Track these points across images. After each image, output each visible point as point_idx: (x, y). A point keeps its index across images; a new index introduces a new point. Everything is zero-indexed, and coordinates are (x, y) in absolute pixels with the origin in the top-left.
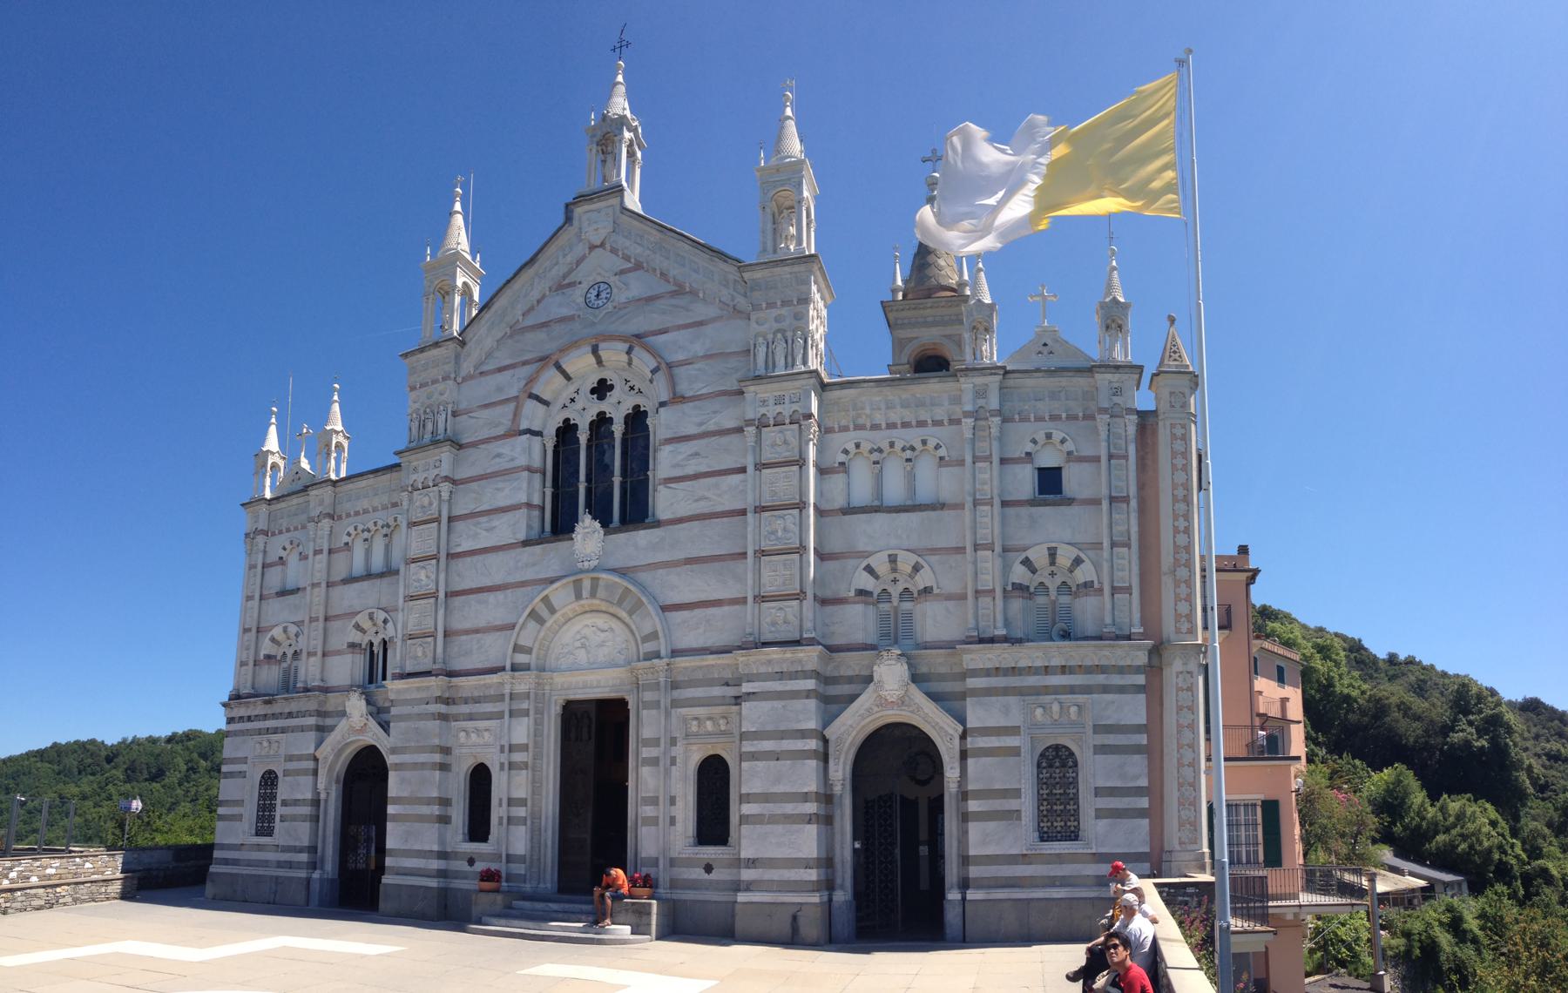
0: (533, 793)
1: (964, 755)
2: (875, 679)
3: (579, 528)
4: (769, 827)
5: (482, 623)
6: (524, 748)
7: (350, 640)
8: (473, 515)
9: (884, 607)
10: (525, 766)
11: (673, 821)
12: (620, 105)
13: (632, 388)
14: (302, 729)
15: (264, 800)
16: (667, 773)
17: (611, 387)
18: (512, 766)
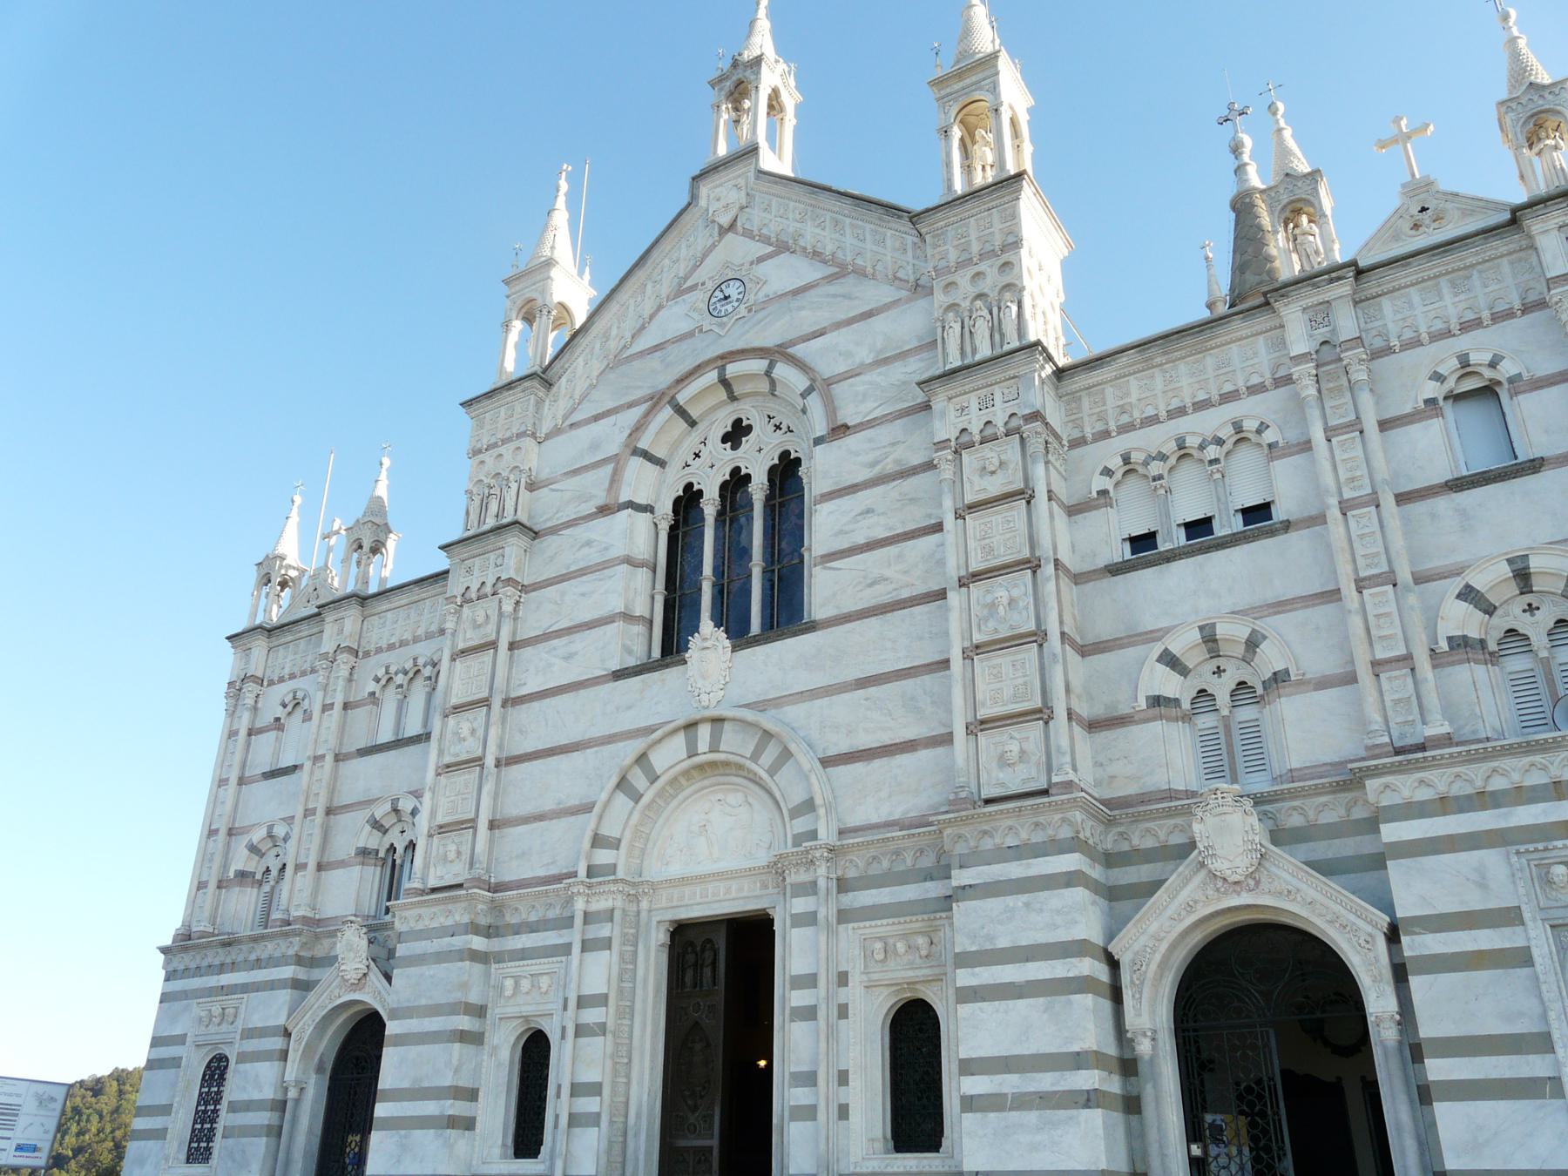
0: (615, 1073)
2: (1200, 846)
3: (695, 642)
5: (549, 805)
6: (602, 1000)
7: (361, 844)
8: (546, 637)
9: (1206, 721)
10: (601, 1029)
11: (843, 1112)
12: (762, 41)
13: (778, 427)
14: (272, 985)
15: (206, 1104)
16: (832, 1035)
17: (749, 428)
18: (580, 1031)
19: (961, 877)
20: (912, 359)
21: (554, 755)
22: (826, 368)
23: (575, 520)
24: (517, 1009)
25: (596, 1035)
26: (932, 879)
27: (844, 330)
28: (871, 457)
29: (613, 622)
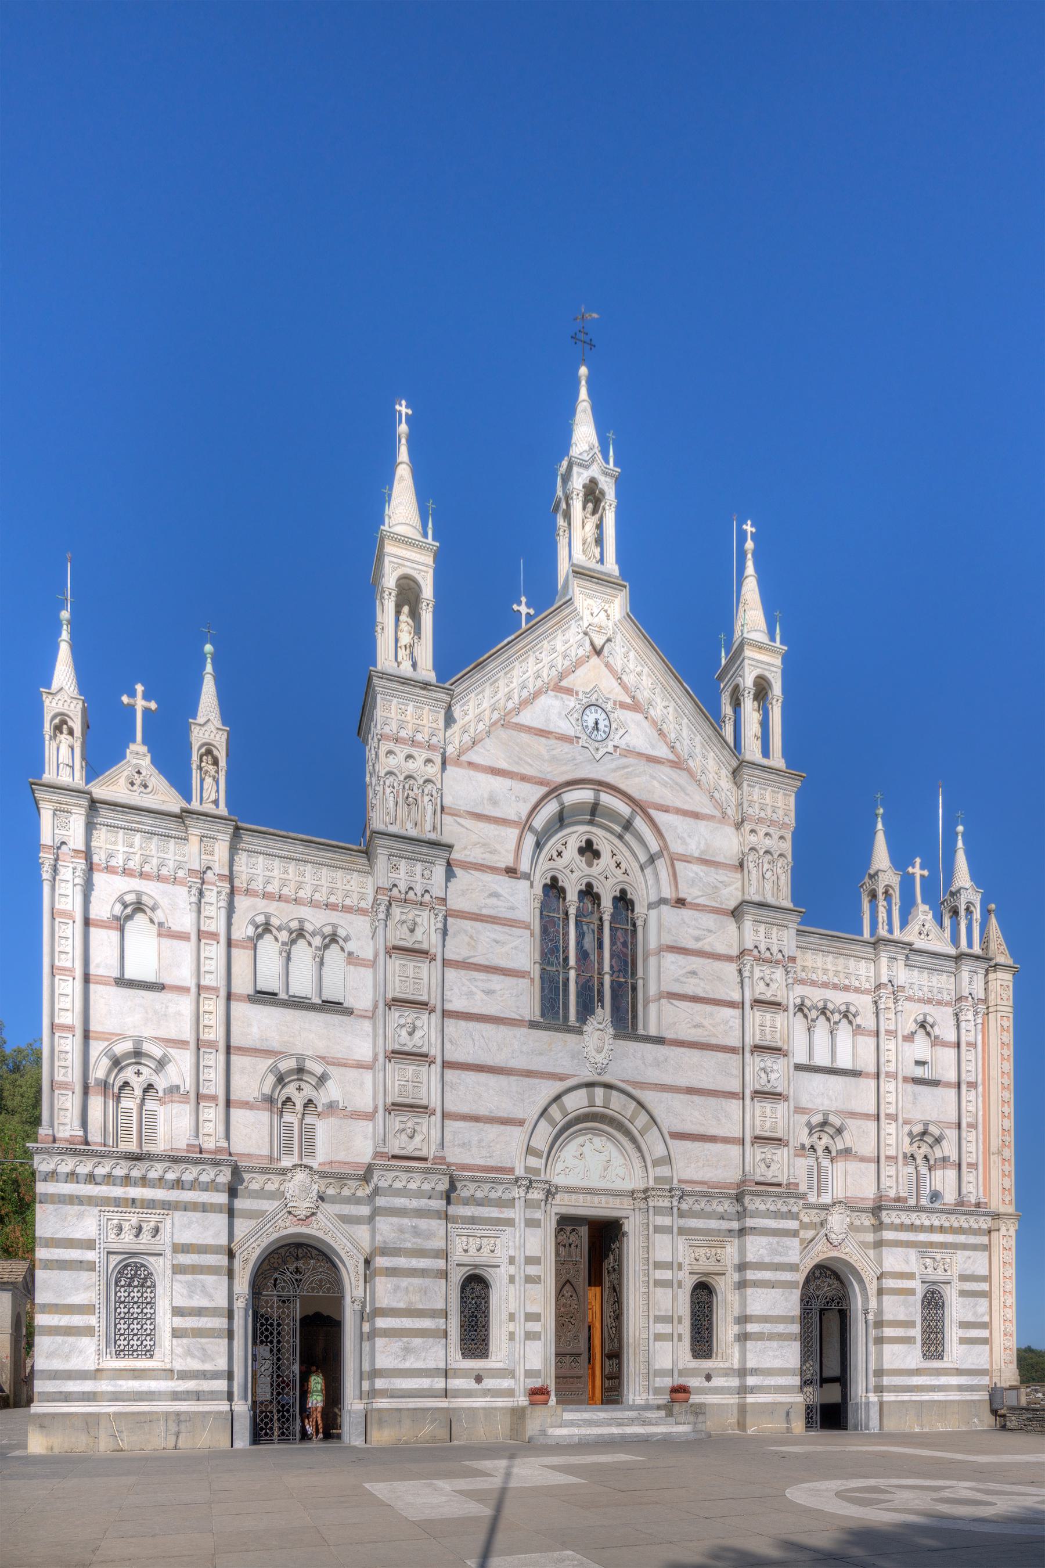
1: (880, 1292)
4: (767, 1343)
5: (483, 1111)
19: (750, 1222)
20: (721, 871)
21: (483, 1071)
22: (676, 847)
23: (481, 865)
24: (472, 1259)
25: (536, 1283)
26: (723, 1219)
27: (681, 818)
28: (697, 933)
29: (524, 977)
